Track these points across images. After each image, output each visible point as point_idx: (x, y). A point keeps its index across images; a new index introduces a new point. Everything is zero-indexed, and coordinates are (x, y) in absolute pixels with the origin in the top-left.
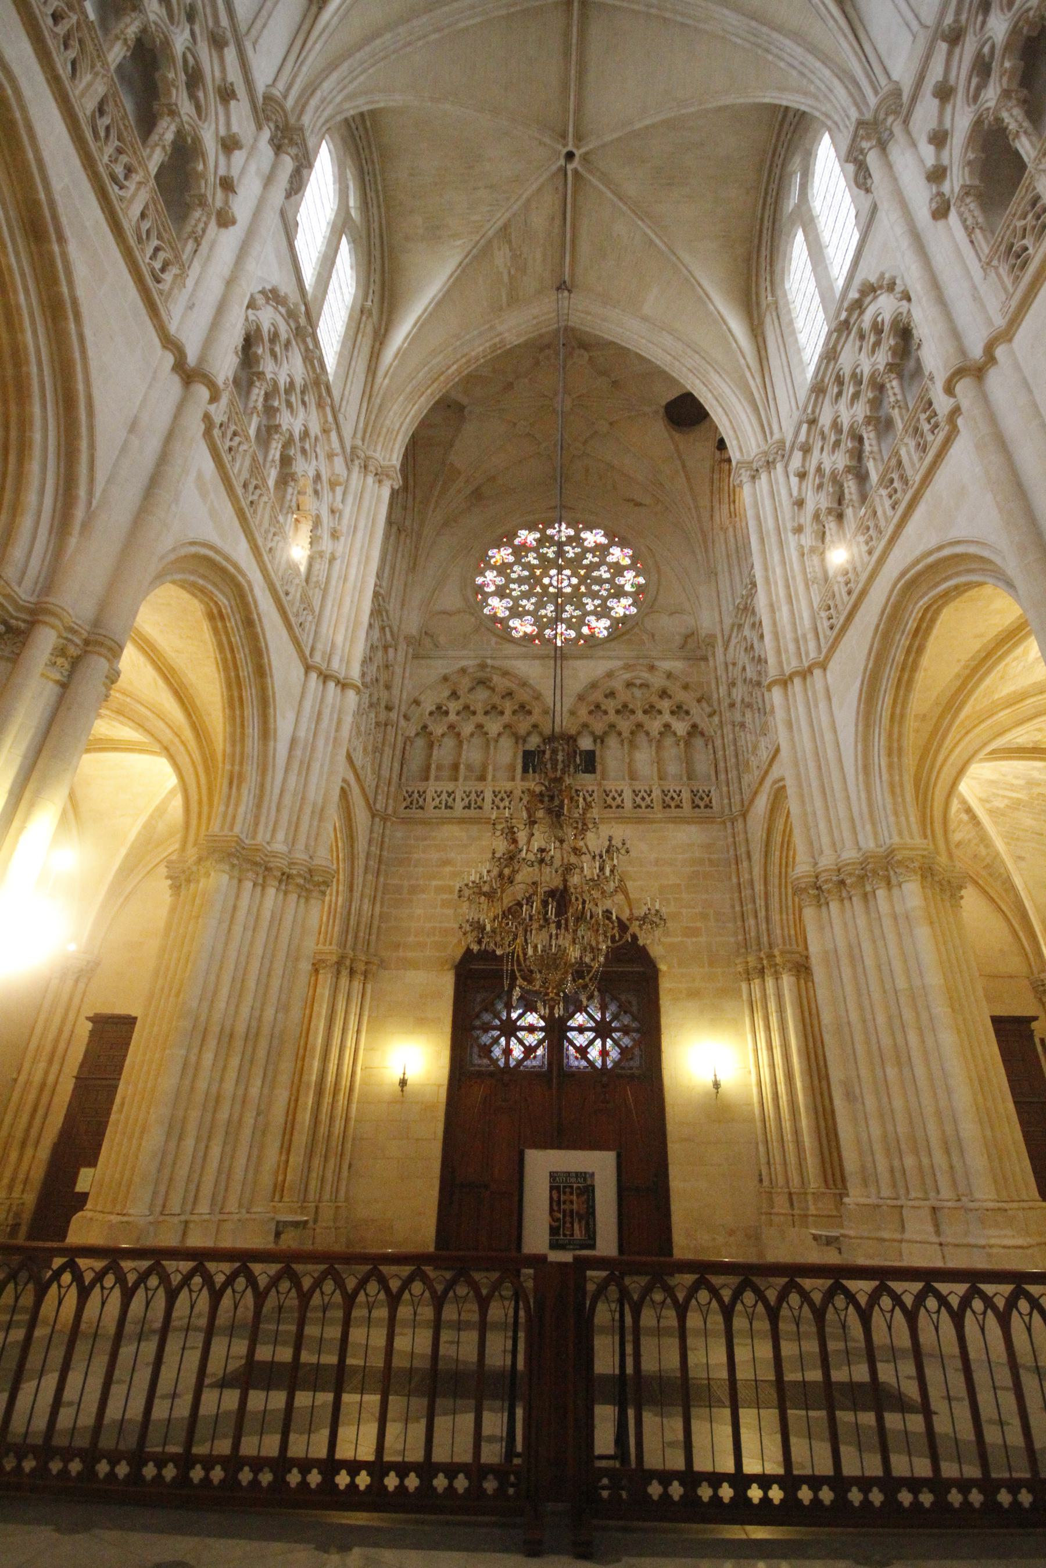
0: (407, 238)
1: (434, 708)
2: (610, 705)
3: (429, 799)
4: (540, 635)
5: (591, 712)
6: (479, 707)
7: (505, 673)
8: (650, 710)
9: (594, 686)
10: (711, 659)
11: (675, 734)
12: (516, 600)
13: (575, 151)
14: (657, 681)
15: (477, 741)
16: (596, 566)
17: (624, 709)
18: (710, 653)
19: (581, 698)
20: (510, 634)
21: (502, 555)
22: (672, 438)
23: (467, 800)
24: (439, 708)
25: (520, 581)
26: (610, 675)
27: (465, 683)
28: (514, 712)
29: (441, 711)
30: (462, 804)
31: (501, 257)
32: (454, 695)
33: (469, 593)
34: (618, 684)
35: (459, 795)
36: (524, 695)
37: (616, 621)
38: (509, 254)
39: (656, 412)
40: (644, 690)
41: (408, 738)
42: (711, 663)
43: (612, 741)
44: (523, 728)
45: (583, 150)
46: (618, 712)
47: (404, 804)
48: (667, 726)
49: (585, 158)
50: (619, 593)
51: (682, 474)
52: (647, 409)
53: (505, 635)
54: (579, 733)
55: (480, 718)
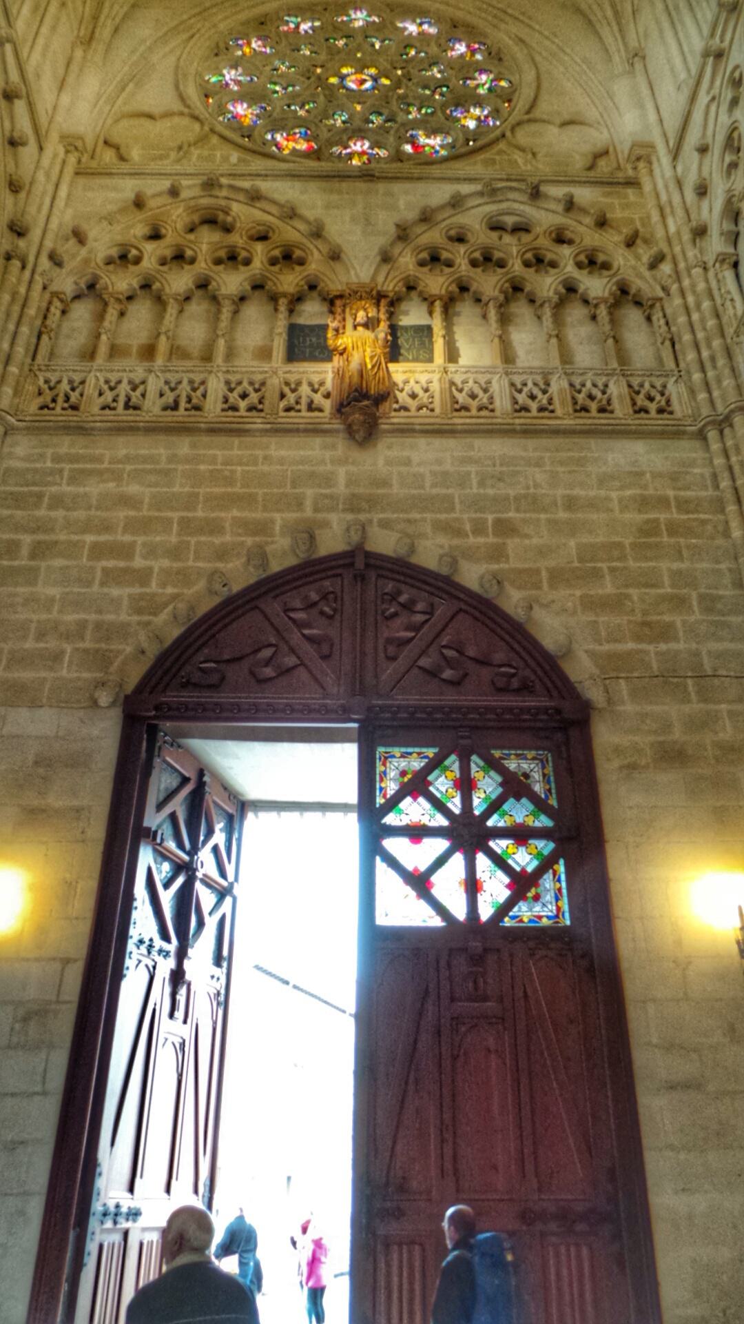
1: (114, 252)
3: (90, 389)
7: (255, 197)
8: (539, 262)
9: (426, 217)
14: (545, 218)
15: (198, 307)
19: (403, 234)
23: (170, 398)
24: (123, 257)
26: (456, 203)
27: (177, 217)
29: (124, 258)
34: (473, 219)
35: (154, 385)
36: (291, 233)
41: (55, 294)
42: (647, 187)
47: (40, 401)
55: (202, 266)
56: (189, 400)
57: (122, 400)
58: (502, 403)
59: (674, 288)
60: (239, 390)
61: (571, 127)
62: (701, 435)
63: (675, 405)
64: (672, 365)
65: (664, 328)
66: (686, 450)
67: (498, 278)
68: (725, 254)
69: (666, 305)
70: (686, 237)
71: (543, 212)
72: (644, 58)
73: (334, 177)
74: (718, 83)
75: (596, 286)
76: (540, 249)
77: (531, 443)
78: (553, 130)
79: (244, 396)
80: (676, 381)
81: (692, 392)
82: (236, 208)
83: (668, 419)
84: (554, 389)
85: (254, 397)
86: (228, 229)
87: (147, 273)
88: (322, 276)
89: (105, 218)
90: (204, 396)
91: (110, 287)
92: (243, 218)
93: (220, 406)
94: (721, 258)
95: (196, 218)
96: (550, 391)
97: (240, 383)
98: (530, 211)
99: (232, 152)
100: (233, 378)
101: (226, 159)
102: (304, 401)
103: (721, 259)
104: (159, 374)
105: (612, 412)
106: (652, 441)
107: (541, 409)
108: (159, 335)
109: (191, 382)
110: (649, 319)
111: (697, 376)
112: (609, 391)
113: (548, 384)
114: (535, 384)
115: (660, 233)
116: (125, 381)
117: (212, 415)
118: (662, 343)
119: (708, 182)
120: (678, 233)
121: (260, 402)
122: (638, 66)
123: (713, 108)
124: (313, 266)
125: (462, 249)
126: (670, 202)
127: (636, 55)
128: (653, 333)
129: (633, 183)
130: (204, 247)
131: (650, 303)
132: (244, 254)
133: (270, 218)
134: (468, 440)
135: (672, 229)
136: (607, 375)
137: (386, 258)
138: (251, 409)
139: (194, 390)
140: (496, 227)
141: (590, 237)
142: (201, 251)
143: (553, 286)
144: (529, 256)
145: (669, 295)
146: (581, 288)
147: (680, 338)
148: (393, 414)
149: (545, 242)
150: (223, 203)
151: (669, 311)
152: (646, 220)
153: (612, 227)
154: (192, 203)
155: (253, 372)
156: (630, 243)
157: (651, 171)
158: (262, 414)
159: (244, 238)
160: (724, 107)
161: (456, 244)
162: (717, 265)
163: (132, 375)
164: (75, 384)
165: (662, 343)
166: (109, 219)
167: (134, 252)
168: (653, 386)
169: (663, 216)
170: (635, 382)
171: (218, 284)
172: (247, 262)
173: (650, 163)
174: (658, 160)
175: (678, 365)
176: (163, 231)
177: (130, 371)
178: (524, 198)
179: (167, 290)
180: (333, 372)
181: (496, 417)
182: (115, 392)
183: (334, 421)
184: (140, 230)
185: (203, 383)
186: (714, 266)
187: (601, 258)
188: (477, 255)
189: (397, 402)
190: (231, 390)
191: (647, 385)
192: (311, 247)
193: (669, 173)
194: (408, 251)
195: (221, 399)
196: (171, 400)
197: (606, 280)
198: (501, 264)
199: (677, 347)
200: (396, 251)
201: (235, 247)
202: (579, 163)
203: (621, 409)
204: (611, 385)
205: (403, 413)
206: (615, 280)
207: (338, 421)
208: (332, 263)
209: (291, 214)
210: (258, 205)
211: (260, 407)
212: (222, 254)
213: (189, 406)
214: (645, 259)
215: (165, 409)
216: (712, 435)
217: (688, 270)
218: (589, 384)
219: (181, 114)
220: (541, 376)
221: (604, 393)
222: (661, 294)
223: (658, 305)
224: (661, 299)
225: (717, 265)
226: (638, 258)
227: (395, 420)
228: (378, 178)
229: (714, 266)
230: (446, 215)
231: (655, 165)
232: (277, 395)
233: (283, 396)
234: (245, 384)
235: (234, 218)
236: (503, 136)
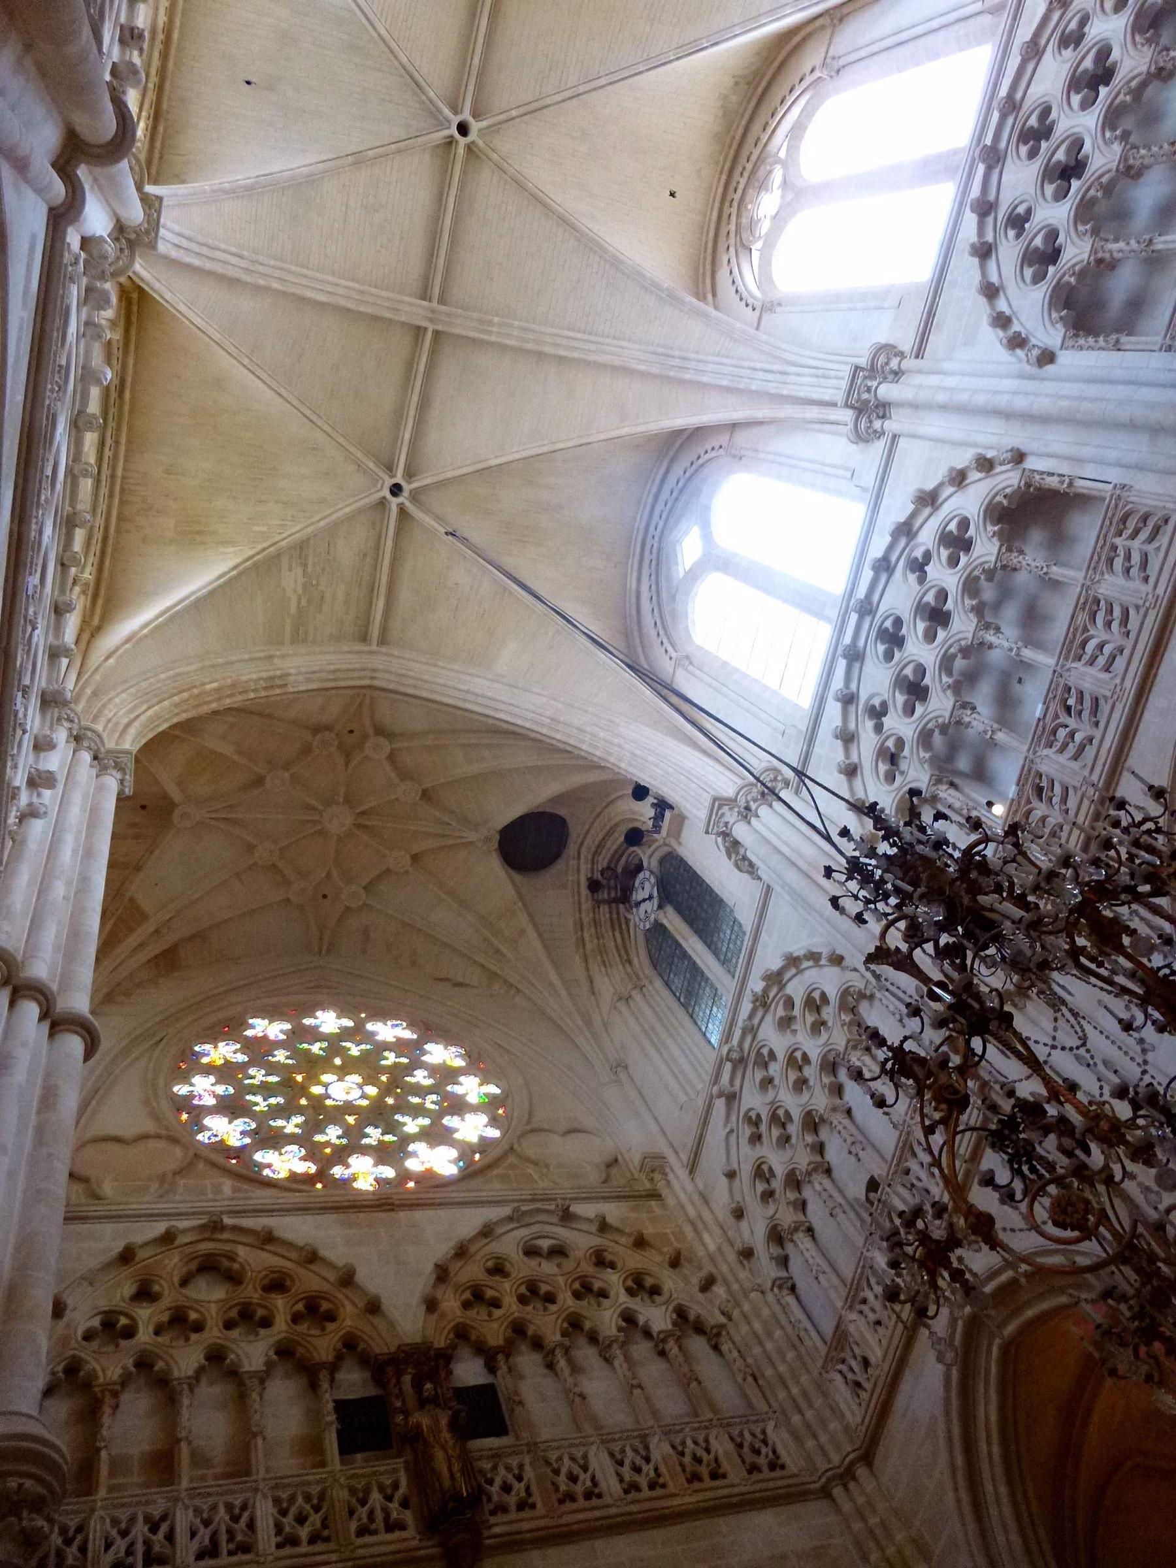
0: (144, 540)
1: (96, 1322)
2: (507, 1291)
4: (321, 1175)
5: (466, 1305)
6: (213, 1316)
7: (268, 1239)
8: (585, 1290)
9: (461, 1252)
10: (665, 1193)
11: (647, 1333)
12: (262, 1119)
13: (404, 484)
14: (581, 1241)
15: (212, 1391)
16: (410, 1069)
17: (533, 1293)
18: (661, 1185)
19: (442, 1274)
20: (259, 1173)
21: (222, 1052)
22: (513, 882)
23: (204, 1535)
25: (266, 1090)
26: (487, 1232)
27: (173, 1264)
28: (296, 1319)
30: (195, 1546)
31: (291, 580)
32: (145, 1294)
33: (165, 1107)
34: (509, 1245)
35: (183, 1520)
36: (310, 1281)
37: (466, 1151)
38: (301, 580)
39: (488, 840)
40: (559, 1259)
42: (671, 1201)
43: (527, 1361)
44: (324, 1345)
45: (414, 485)
46: (522, 1300)
48: (629, 1318)
49: (415, 496)
50: (458, 1106)
51: (532, 934)
52: (473, 836)
53: (253, 1177)
54: (453, 1347)
55: (214, 1333)
56: (231, 1536)
57: (140, 1549)
58: (611, 1485)
59: (736, 1314)
60: (293, 1511)
61: (573, 1135)
62: (825, 1493)
63: (785, 1458)
64: (761, 1406)
65: (739, 1363)
66: (815, 1514)
67: (554, 1317)
68: (780, 1278)
69: (732, 1332)
70: (732, 1257)
71: (576, 1233)
72: (626, 1067)
73: (350, 1207)
74: (734, 1118)
75: (657, 1317)
76: (585, 1276)
77: (658, 1535)
78: (557, 1138)
79: (301, 1520)
80: (776, 1426)
81: (797, 1438)
82: (242, 1252)
83: (782, 1478)
84: (656, 1455)
85: (315, 1519)
86: (234, 1278)
87: (143, 1351)
88: (359, 1333)
89: (85, 1279)
90: (251, 1525)
91: (100, 1374)
92: (251, 1261)
93: (274, 1540)
94: (778, 1283)
95: (193, 1266)
96: (652, 1457)
97: (292, 1499)
98: (563, 1233)
99: (222, 1180)
100: (284, 1495)
101: (217, 1189)
102: (379, 1515)
103: (779, 1284)
104: (187, 1501)
105: (724, 1476)
106: (779, 1509)
107: (652, 1486)
108: (179, 1441)
109: (229, 1507)
110: (716, 1348)
111: (796, 1419)
112: (713, 1450)
113: (647, 1448)
114: (635, 1451)
115: (701, 1253)
116: (141, 1518)
117: (270, 1558)
118: (744, 1380)
119: (742, 1204)
120: (719, 1249)
121: (325, 1526)
122: (623, 1075)
123: (733, 1138)
124: (348, 1322)
125: (507, 1285)
126: (701, 1218)
127: (619, 1065)
128: (728, 1365)
129: (654, 1195)
130: (213, 1308)
131: (715, 1331)
132: (260, 1312)
133: (289, 1264)
134: (588, 1544)
135: (712, 1247)
136: (707, 1428)
137: (431, 1305)
138: (313, 1540)
139: (235, 1519)
140: (531, 1252)
141: (634, 1260)
142: (209, 1312)
143: (613, 1323)
144: (577, 1286)
145: (730, 1319)
146: (641, 1320)
147: (763, 1376)
148: (493, 1520)
149: (588, 1268)
150: (227, 1247)
151: (737, 1339)
152: (680, 1235)
153: (652, 1247)
154: (188, 1250)
155: (309, 1483)
156: (675, 1263)
157: (668, 1182)
158: (332, 1545)
159: (260, 1291)
160: (744, 1141)
161: (497, 1278)
162: (775, 1289)
163: (149, 1509)
164: (71, 1533)
165: (744, 1380)
166: (89, 1279)
167: (123, 1321)
168: (753, 1435)
169: (696, 1231)
170: (735, 1432)
171: (238, 1356)
172: (266, 1323)
173: (665, 1174)
174: (672, 1170)
175: (770, 1406)
176: (156, 1288)
177: (147, 1503)
178: (555, 1220)
179: (176, 1374)
180: (407, 1469)
181: (608, 1506)
182: (128, 1539)
183: (424, 1544)
184: (129, 1289)
185: (244, 1507)
186: (772, 1289)
187: (649, 1282)
188: (523, 1289)
189: (489, 1500)
190: (284, 1513)
191: (747, 1435)
192: (341, 1296)
193: (690, 1188)
194: (450, 1293)
195: (272, 1531)
196: (207, 1541)
197: (664, 1308)
198: (550, 1298)
199: (761, 1382)
200: (439, 1294)
201: (249, 1304)
202: (593, 1177)
203: (735, 1472)
204: (712, 1440)
205: (500, 1518)
206: (671, 1308)
207: (430, 1543)
208: (370, 1317)
209: (312, 1257)
210: (267, 1247)
211: (326, 1533)
212: (234, 1313)
213: (232, 1546)
214: (695, 1281)
215: (200, 1557)
216: (837, 1492)
217: (746, 1294)
218: (689, 1442)
219: (158, 1137)
220: (638, 1440)
221: (708, 1451)
222: (723, 1320)
223: (724, 1333)
224: (723, 1326)
225: (775, 1289)
226: (686, 1279)
227: (497, 1530)
228: (398, 1206)
229: (772, 1289)
230: (478, 1245)
231: (671, 1176)
232: (345, 1513)
233: (352, 1512)
234: (300, 1500)
235: (240, 1263)
236: (512, 1148)
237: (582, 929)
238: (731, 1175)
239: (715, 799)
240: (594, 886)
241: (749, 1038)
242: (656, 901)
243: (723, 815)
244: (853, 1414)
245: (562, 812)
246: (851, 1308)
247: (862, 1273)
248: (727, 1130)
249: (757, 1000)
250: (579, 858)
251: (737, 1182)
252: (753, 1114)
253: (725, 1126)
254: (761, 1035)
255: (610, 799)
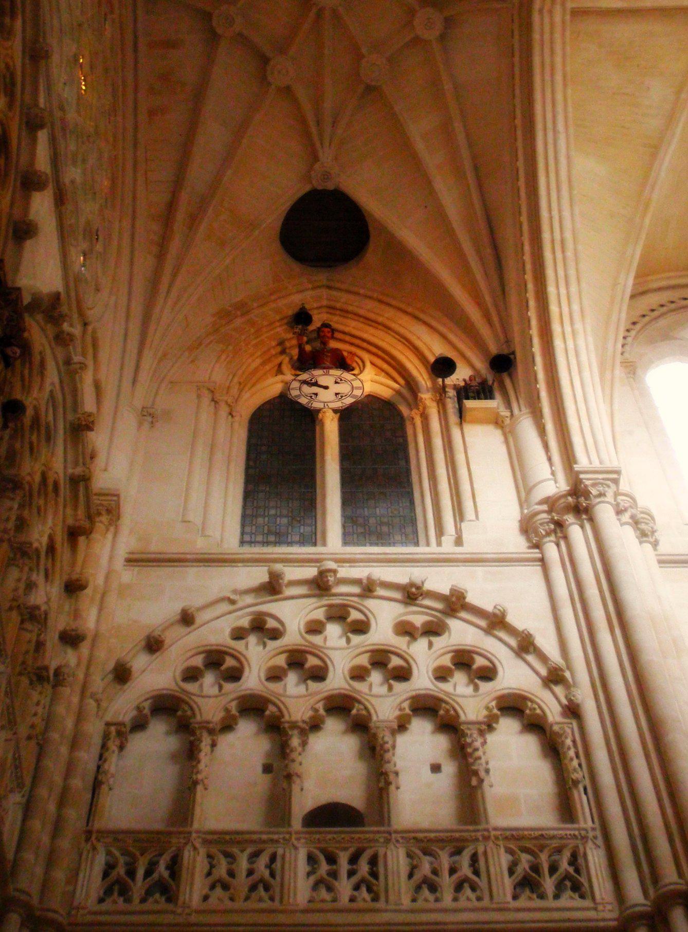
39: (327, 176)
74: (249, 599)
162: (113, 729)
186: (108, 724)
237: (243, 315)
238: (187, 619)
239: (618, 472)
240: (302, 318)
241: (356, 590)
242: (338, 405)
243: (609, 486)
244: (87, 895)
245: (372, 256)
246: (206, 842)
247: (264, 842)
248: (233, 597)
249: (418, 588)
250: (314, 288)
251: (183, 630)
252: (271, 624)
253: (235, 591)
254: (371, 603)
255: (422, 316)
